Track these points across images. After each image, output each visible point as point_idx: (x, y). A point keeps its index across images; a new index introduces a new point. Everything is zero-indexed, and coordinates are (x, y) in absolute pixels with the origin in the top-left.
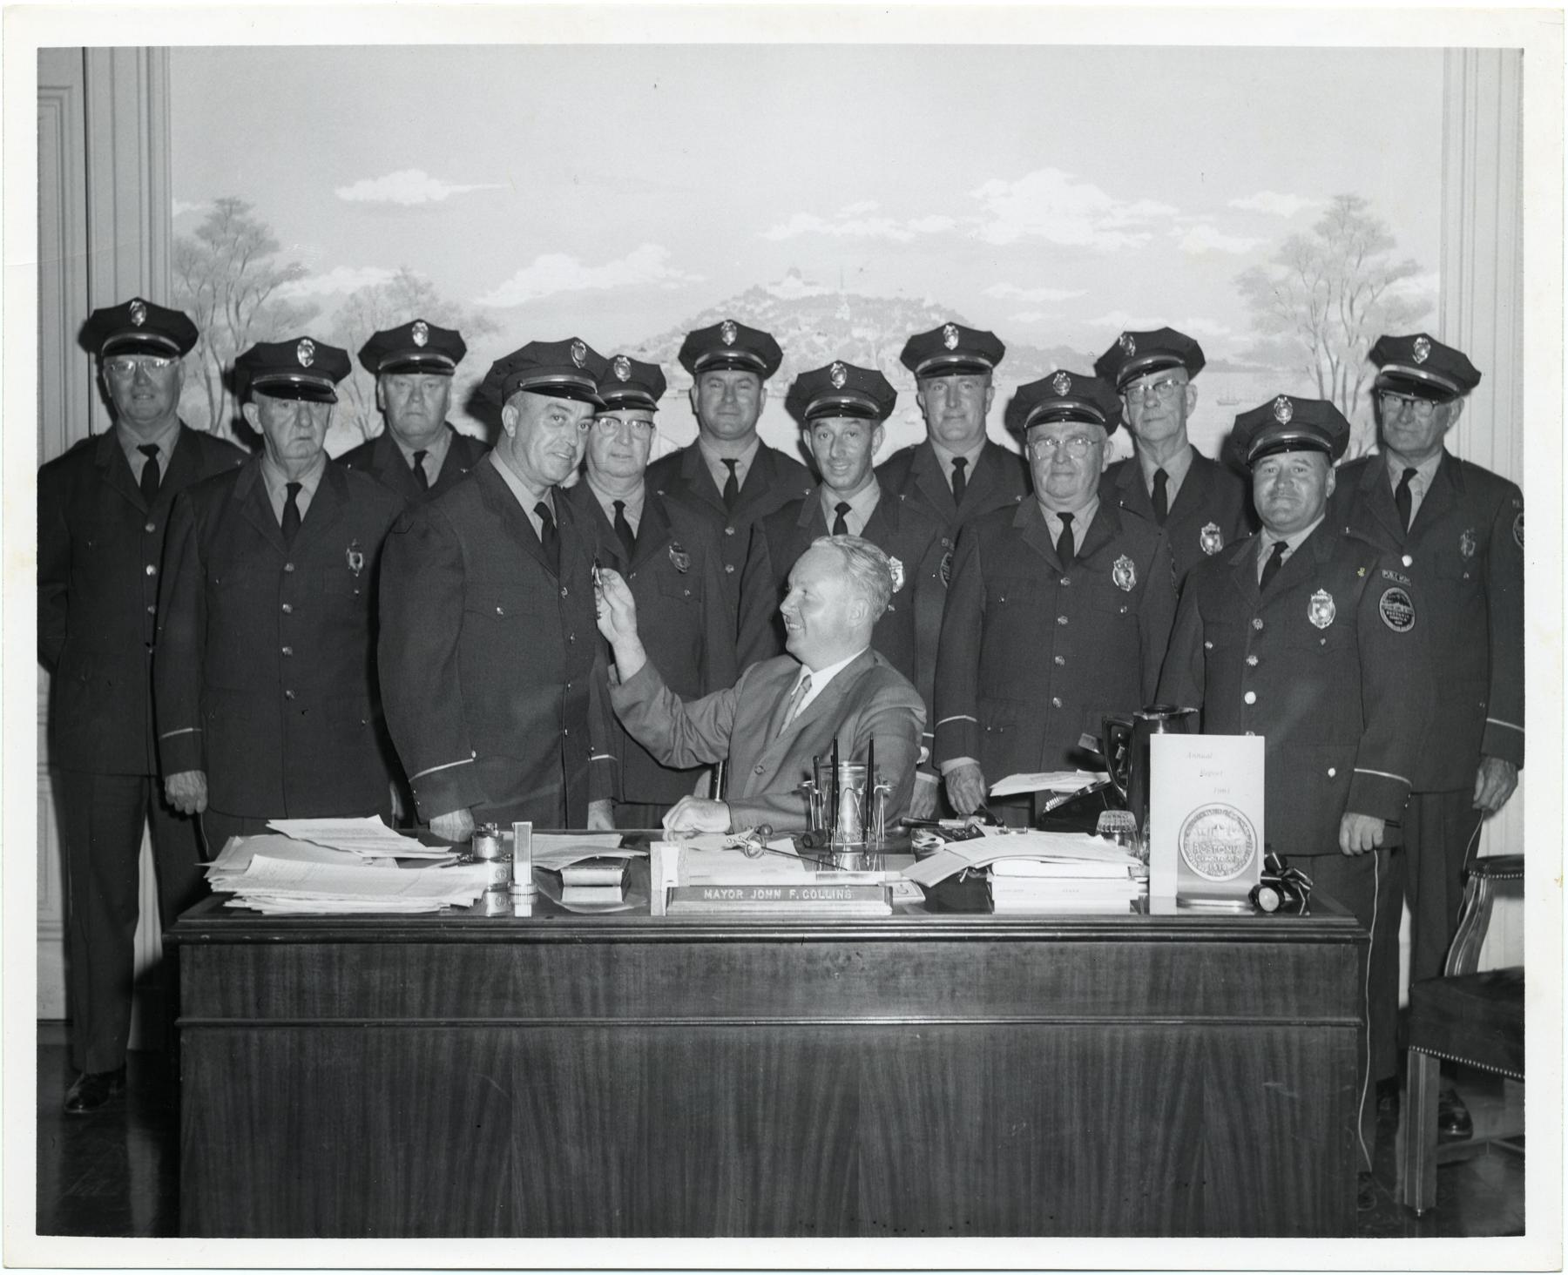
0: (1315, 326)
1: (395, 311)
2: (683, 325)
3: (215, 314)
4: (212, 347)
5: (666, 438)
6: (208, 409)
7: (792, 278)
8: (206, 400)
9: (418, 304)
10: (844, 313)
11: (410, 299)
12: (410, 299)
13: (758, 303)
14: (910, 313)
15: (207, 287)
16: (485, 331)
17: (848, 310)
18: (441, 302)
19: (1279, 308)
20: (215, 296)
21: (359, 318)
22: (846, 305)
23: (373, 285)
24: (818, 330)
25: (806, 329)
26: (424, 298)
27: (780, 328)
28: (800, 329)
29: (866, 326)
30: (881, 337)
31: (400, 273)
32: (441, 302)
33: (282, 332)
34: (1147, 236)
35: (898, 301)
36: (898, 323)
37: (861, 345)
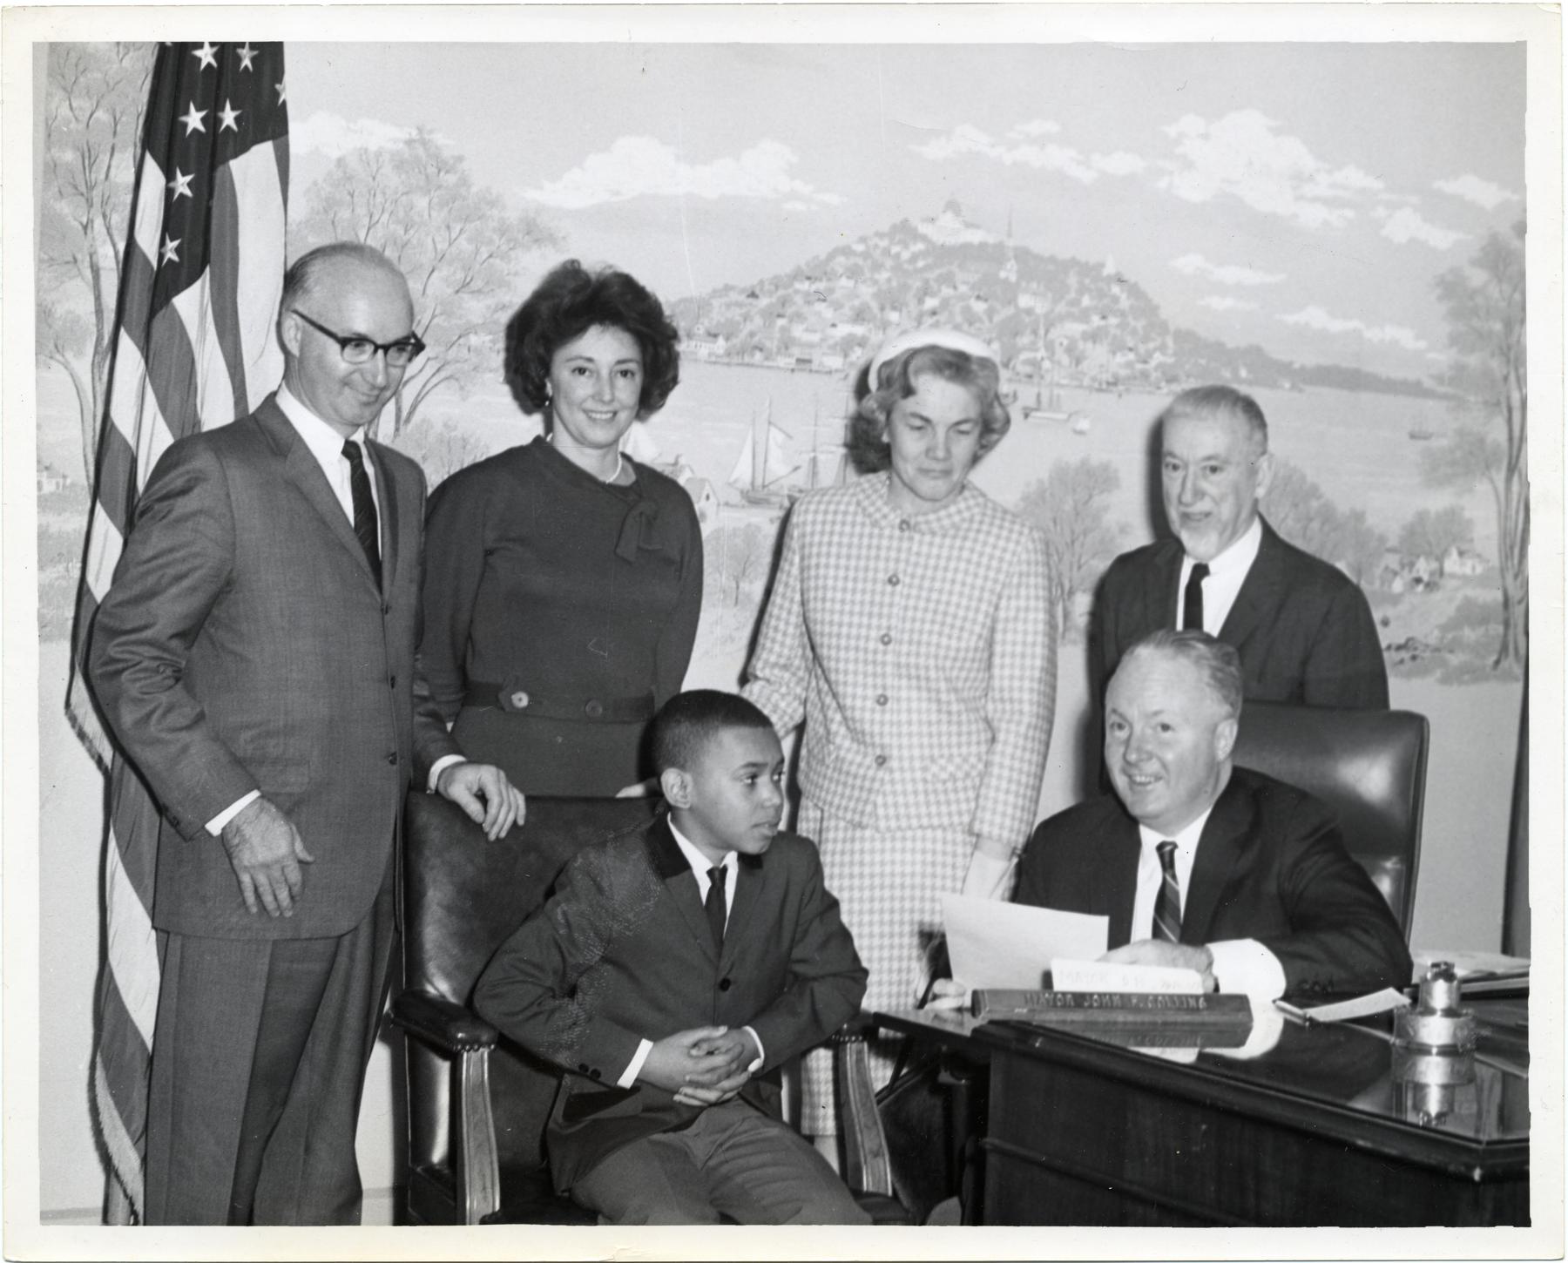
0: (1509, 348)
1: (407, 193)
2: (807, 264)
3: (114, 163)
4: (104, 216)
5: (776, 426)
6: (93, 319)
7: (949, 215)
8: (93, 309)
10: (1009, 272)
11: (427, 177)
12: (427, 177)
13: (906, 246)
14: (1087, 281)
15: (102, 115)
16: (536, 241)
17: (1015, 268)
18: (474, 189)
19: (1475, 323)
20: (115, 133)
21: (348, 198)
22: (1013, 262)
23: (373, 148)
24: (976, 293)
25: (963, 289)
26: (451, 179)
27: (932, 283)
28: (955, 288)
29: (1035, 294)
30: (1052, 311)
31: (414, 134)
34: (1349, 213)
35: (1074, 262)
36: (1072, 295)
37: (1027, 320)
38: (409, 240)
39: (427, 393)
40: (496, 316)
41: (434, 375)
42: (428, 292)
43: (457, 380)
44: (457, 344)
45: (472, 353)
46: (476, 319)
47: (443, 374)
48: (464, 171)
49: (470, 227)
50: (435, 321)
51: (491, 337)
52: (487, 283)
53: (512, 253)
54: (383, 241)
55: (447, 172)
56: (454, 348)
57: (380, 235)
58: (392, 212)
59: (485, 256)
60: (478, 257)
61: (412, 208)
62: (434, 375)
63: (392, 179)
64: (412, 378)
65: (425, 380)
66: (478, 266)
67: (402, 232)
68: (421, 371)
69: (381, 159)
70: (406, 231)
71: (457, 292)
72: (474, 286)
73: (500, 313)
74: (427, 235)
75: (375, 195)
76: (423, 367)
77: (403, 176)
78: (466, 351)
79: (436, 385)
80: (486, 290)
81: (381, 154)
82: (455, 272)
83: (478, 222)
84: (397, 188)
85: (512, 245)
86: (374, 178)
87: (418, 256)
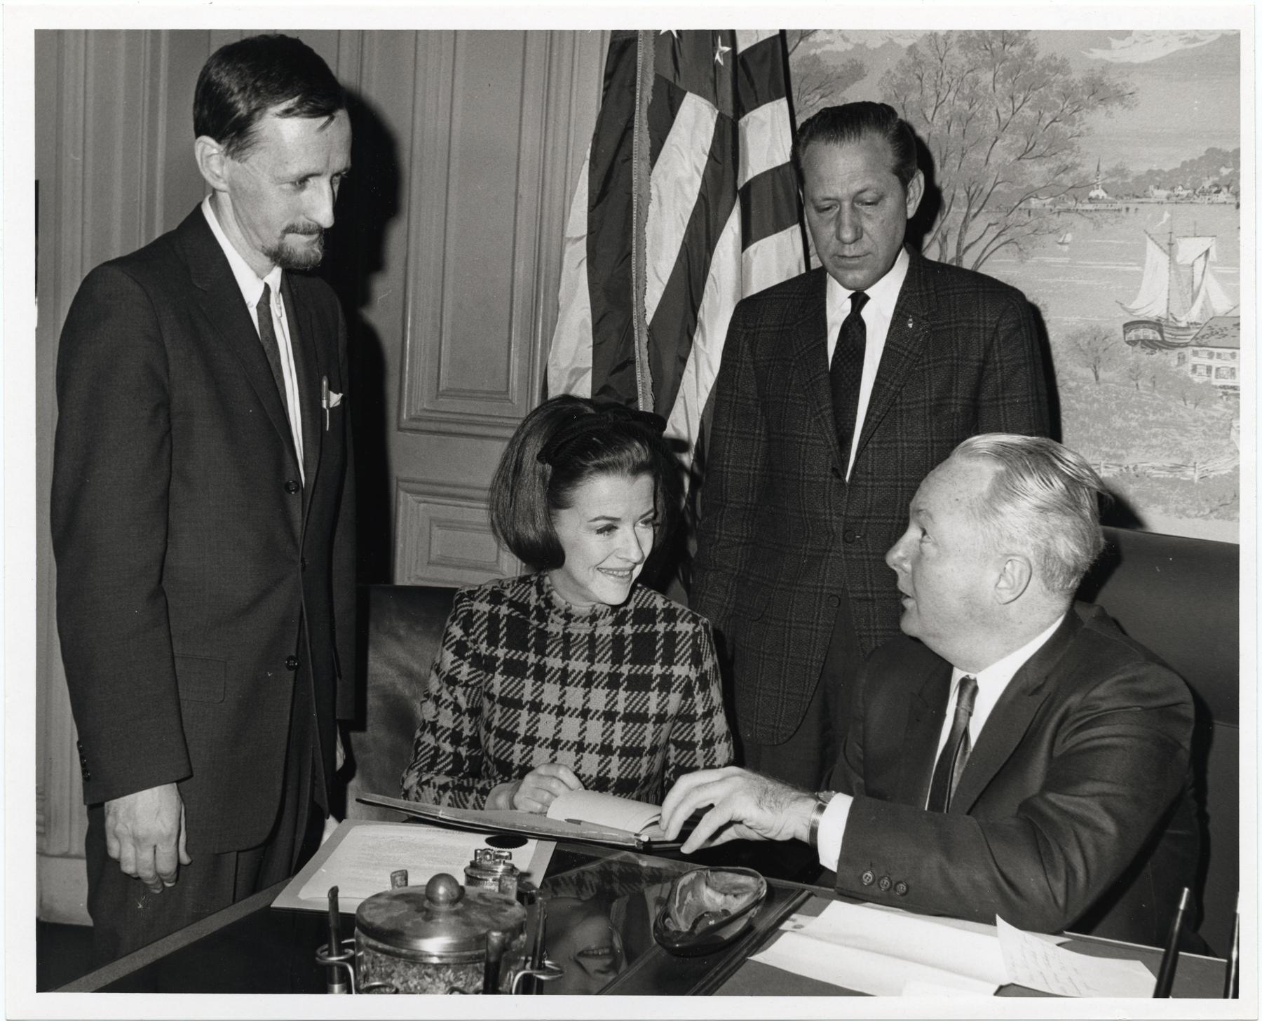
1: (972, 71)
9: (1004, 60)
12: (992, 53)
16: (1102, 100)
18: (1036, 59)
21: (918, 82)
26: (1016, 50)
32: (1039, 57)
33: (810, 103)
38: (973, 114)
39: (985, 259)
40: (1057, 178)
41: (994, 239)
42: (991, 161)
43: (1016, 243)
44: (1017, 208)
45: (1032, 217)
46: (1037, 183)
47: (1002, 239)
48: (1029, 41)
49: (1034, 96)
50: (996, 189)
51: (1052, 199)
52: (1050, 147)
53: (1076, 114)
54: (948, 118)
55: (1011, 45)
56: (1015, 213)
57: (946, 113)
58: (958, 90)
59: (1047, 122)
60: (1041, 123)
61: (977, 84)
62: (994, 239)
63: (958, 58)
64: (973, 244)
65: (985, 246)
66: (1041, 132)
67: (968, 108)
68: (981, 237)
69: (949, 42)
70: (970, 108)
71: (1019, 159)
72: (1036, 151)
73: (1062, 175)
74: (990, 107)
75: (942, 75)
76: (984, 234)
77: (970, 55)
78: (1027, 216)
79: (995, 250)
80: (1048, 153)
81: (949, 38)
82: (1017, 140)
83: (1042, 89)
84: (963, 66)
85: (1076, 107)
86: (942, 61)
87: (982, 127)
